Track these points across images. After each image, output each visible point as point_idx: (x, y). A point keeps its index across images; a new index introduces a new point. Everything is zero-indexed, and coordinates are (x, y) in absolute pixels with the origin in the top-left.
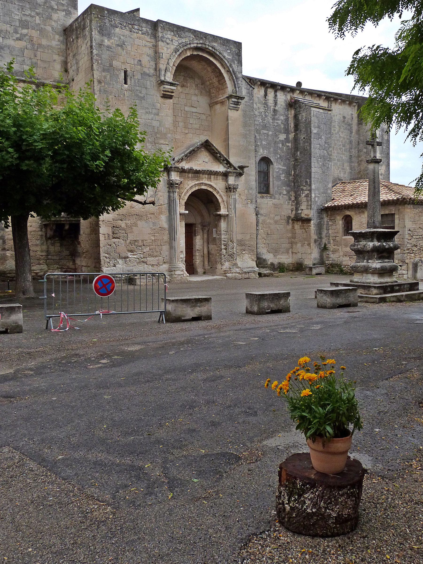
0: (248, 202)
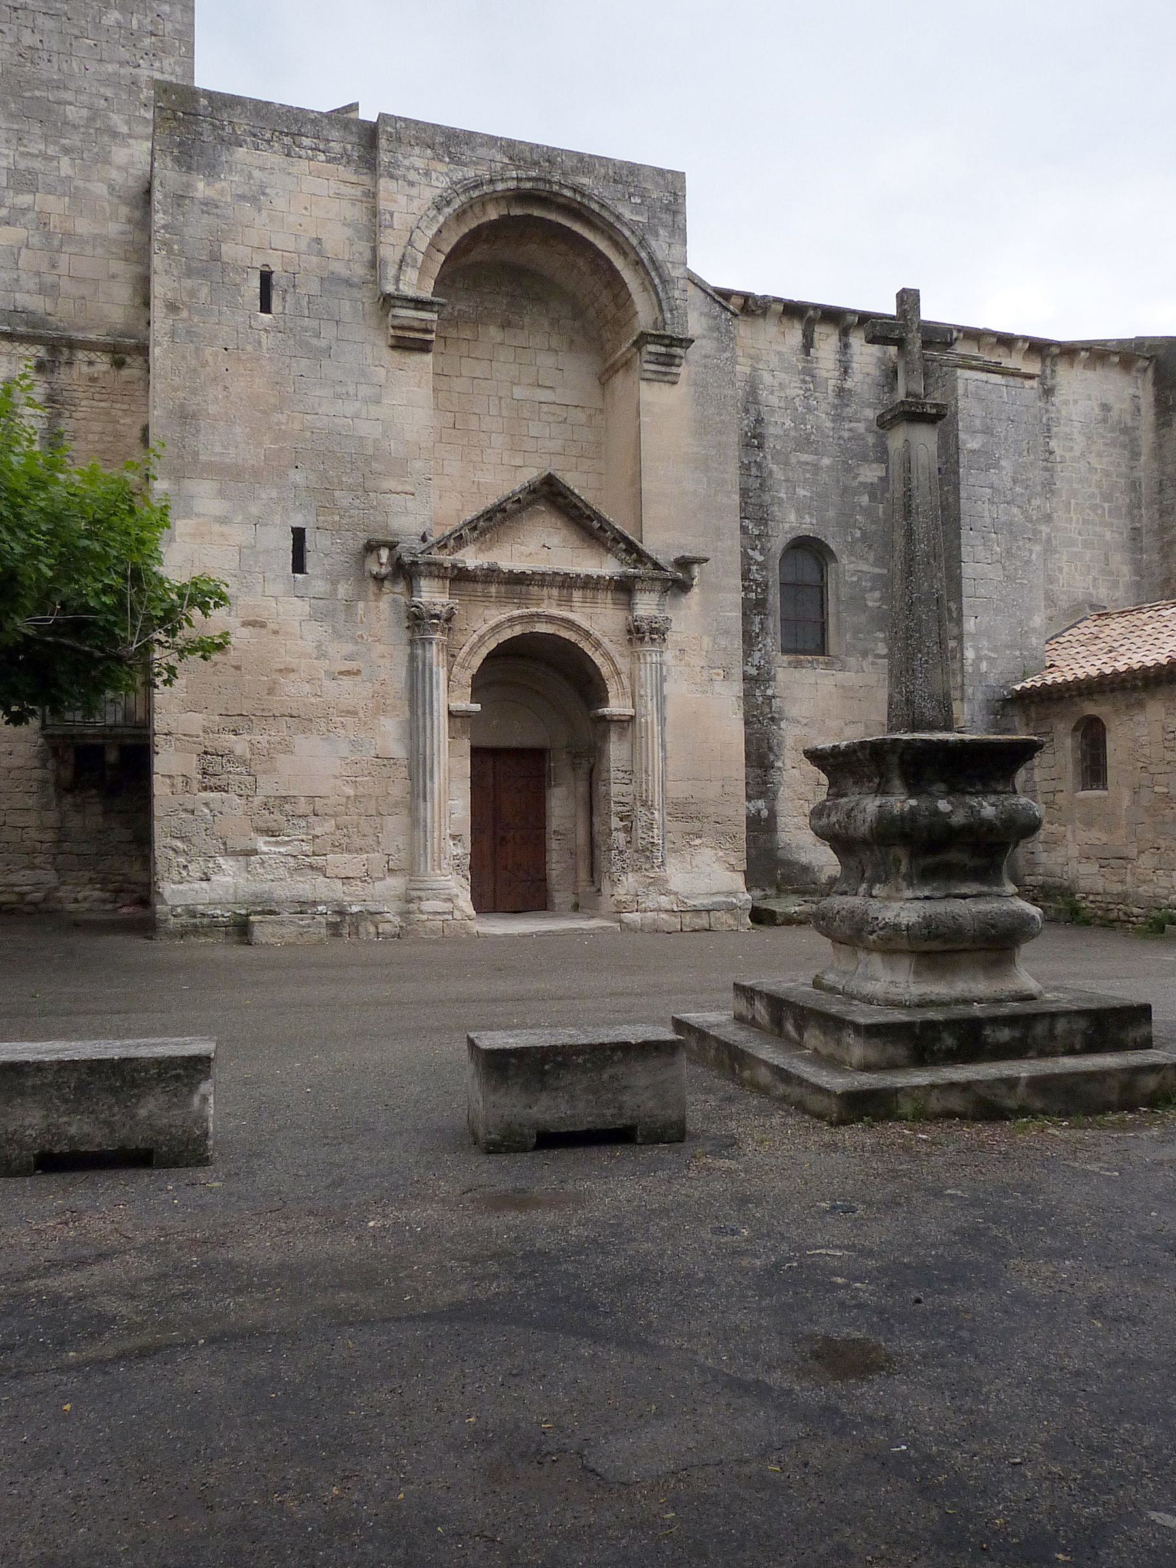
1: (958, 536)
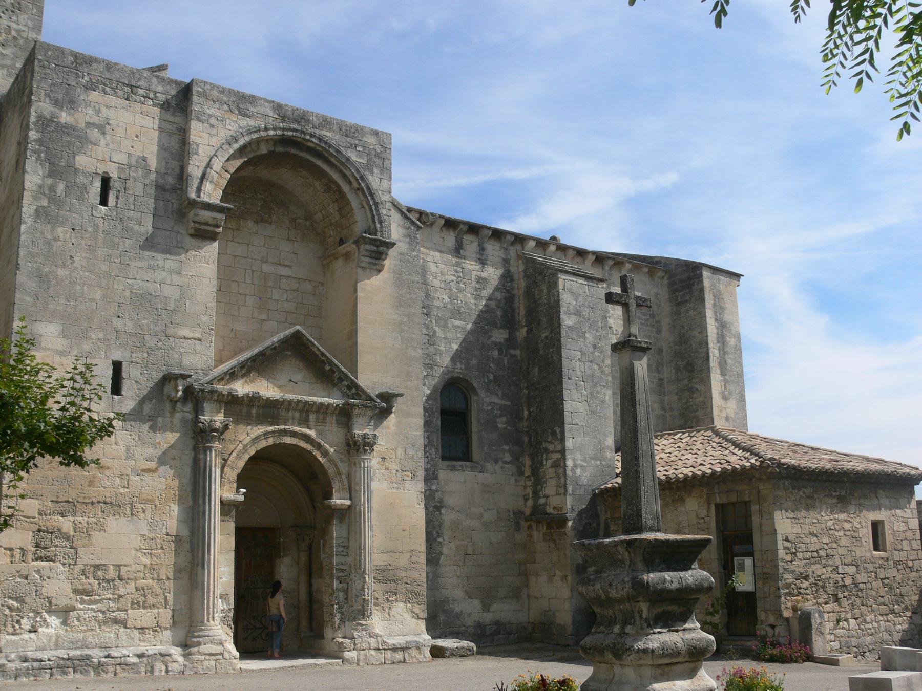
0: (406, 478)
1: (561, 383)
